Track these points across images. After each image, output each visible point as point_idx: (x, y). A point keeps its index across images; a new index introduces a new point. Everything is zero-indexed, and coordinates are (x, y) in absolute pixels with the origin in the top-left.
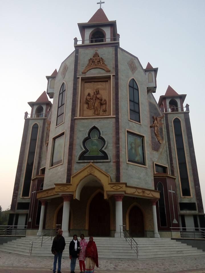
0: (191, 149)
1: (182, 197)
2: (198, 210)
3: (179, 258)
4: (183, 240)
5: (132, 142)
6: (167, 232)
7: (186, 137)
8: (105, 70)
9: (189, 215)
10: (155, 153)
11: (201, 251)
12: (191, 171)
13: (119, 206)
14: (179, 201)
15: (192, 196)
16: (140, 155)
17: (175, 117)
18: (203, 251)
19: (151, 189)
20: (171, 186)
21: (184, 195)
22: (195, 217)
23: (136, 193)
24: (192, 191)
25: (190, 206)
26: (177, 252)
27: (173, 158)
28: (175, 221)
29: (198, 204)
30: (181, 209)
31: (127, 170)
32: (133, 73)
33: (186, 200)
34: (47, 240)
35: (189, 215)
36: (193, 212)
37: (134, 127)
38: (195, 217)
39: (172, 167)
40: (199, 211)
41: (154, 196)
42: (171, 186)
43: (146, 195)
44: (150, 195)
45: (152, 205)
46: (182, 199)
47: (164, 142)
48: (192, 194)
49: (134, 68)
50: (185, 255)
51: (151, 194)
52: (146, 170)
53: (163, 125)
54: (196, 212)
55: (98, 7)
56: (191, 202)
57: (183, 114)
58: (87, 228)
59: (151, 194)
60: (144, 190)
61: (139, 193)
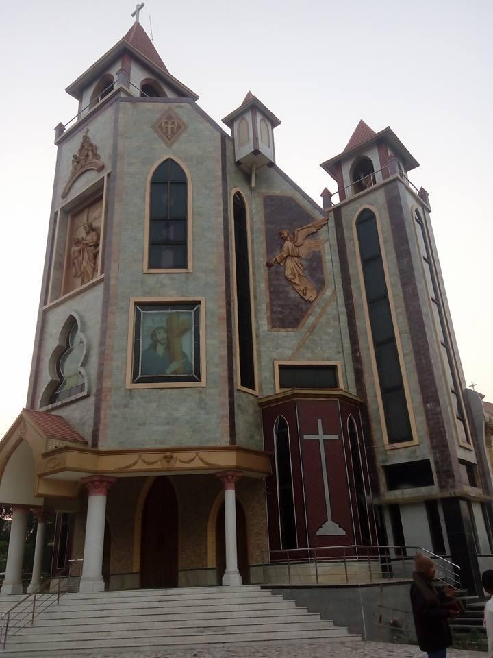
0: (407, 290)
1: (388, 447)
2: (440, 482)
3: (342, 643)
4: (289, 590)
5: (159, 328)
6: (297, 565)
7: (393, 256)
8: (93, 169)
9: (412, 503)
10: (284, 334)
11: (329, 624)
12: (411, 357)
13: (97, 508)
14: (380, 462)
15: (416, 440)
16: (184, 355)
17: (361, 209)
18: (335, 625)
19: (218, 444)
20: (319, 421)
21: (392, 440)
22: (431, 505)
23: (138, 467)
24: (417, 423)
25: (415, 473)
26: (197, 632)
27: (359, 333)
28: (330, 528)
29: (436, 463)
30: (392, 486)
31: (126, 406)
32: (170, 146)
33: (401, 455)
34: (47, 603)
35: (412, 503)
36: (424, 491)
37: (163, 286)
38: (431, 505)
39: (357, 359)
40: (442, 487)
41: (208, 464)
42: (319, 421)
43: (178, 465)
44: (197, 463)
45: (222, 489)
46: (388, 453)
47: (328, 293)
48: (418, 431)
49: (172, 130)
50: (231, 638)
51: (201, 459)
52: (200, 392)
53: (327, 245)
54: (433, 491)
55: (130, 23)
56: (417, 457)
57: (383, 189)
58: (136, 567)
59: (201, 459)
60: (168, 454)
61: (148, 464)
